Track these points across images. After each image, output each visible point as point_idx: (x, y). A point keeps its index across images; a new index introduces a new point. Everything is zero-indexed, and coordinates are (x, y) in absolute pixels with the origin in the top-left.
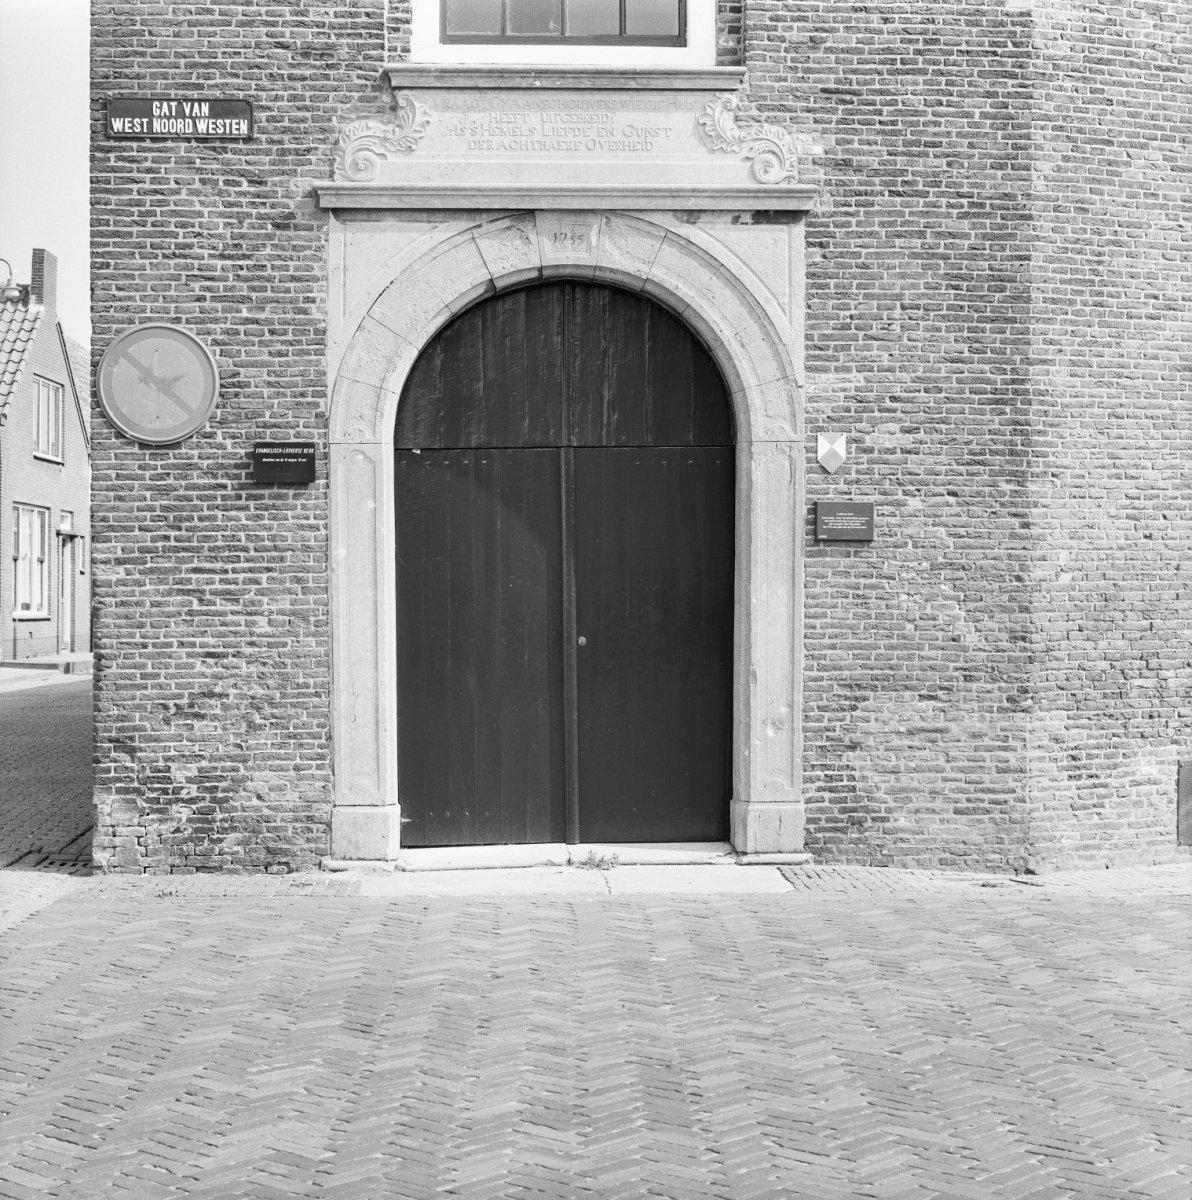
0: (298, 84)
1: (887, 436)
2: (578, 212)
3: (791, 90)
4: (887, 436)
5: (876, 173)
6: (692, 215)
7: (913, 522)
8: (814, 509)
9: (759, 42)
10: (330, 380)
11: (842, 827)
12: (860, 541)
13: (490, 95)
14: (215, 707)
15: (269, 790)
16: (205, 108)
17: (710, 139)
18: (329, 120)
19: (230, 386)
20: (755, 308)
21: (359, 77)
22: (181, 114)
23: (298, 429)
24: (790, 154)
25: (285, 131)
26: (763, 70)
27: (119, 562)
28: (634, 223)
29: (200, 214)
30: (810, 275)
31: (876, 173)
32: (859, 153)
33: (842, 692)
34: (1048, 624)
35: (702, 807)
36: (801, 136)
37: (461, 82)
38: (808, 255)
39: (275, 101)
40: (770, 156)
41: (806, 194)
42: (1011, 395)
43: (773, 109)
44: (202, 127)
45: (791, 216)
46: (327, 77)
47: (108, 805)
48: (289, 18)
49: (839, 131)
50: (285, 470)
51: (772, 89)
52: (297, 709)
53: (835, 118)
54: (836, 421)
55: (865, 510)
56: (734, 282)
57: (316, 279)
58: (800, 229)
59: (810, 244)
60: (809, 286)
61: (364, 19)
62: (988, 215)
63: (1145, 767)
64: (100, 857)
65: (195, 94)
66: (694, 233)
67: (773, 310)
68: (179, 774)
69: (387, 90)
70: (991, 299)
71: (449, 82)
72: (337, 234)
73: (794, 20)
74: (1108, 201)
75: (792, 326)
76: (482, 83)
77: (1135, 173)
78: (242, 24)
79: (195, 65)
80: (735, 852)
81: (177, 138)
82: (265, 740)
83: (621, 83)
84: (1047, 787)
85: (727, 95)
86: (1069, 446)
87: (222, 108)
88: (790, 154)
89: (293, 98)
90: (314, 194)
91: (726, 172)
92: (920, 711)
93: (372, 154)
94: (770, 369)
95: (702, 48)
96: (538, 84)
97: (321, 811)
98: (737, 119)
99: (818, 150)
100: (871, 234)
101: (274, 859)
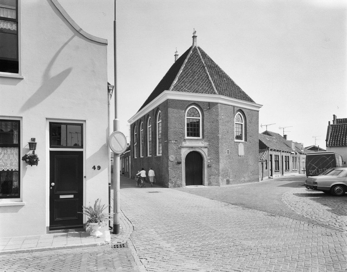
1: (212, 161)
2: (195, 147)
4: (212, 161)
6: (201, 148)
7: (214, 165)
8: (208, 165)
9: (205, 137)
11: (210, 184)
12: (210, 167)
15: (179, 182)
17: (202, 143)
19: (176, 158)
20: (205, 153)
23: (180, 160)
26: (205, 139)
34: (220, 171)
35: (201, 183)
39: (179, 141)
42: (218, 158)
43: (205, 141)
45: (207, 148)
47: (170, 184)
50: (179, 163)
52: (180, 177)
54: (209, 160)
55: (211, 165)
56: (203, 151)
63: (225, 180)
64: (169, 187)
66: (202, 149)
68: (173, 182)
69: (185, 140)
70: (217, 153)
71: (188, 139)
74: (223, 147)
75: (207, 154)
80: (204, 185)
84: (220, 181)
86: (221, 161)
87: (176, 141)
88: (206, 144)
90: (181, 146)
91: (203, 145)
92: (213, 177)
93: (185, 144)
94: (205, 157)
95: (201, 137)
97: (181, 184)
101: (179, 187)
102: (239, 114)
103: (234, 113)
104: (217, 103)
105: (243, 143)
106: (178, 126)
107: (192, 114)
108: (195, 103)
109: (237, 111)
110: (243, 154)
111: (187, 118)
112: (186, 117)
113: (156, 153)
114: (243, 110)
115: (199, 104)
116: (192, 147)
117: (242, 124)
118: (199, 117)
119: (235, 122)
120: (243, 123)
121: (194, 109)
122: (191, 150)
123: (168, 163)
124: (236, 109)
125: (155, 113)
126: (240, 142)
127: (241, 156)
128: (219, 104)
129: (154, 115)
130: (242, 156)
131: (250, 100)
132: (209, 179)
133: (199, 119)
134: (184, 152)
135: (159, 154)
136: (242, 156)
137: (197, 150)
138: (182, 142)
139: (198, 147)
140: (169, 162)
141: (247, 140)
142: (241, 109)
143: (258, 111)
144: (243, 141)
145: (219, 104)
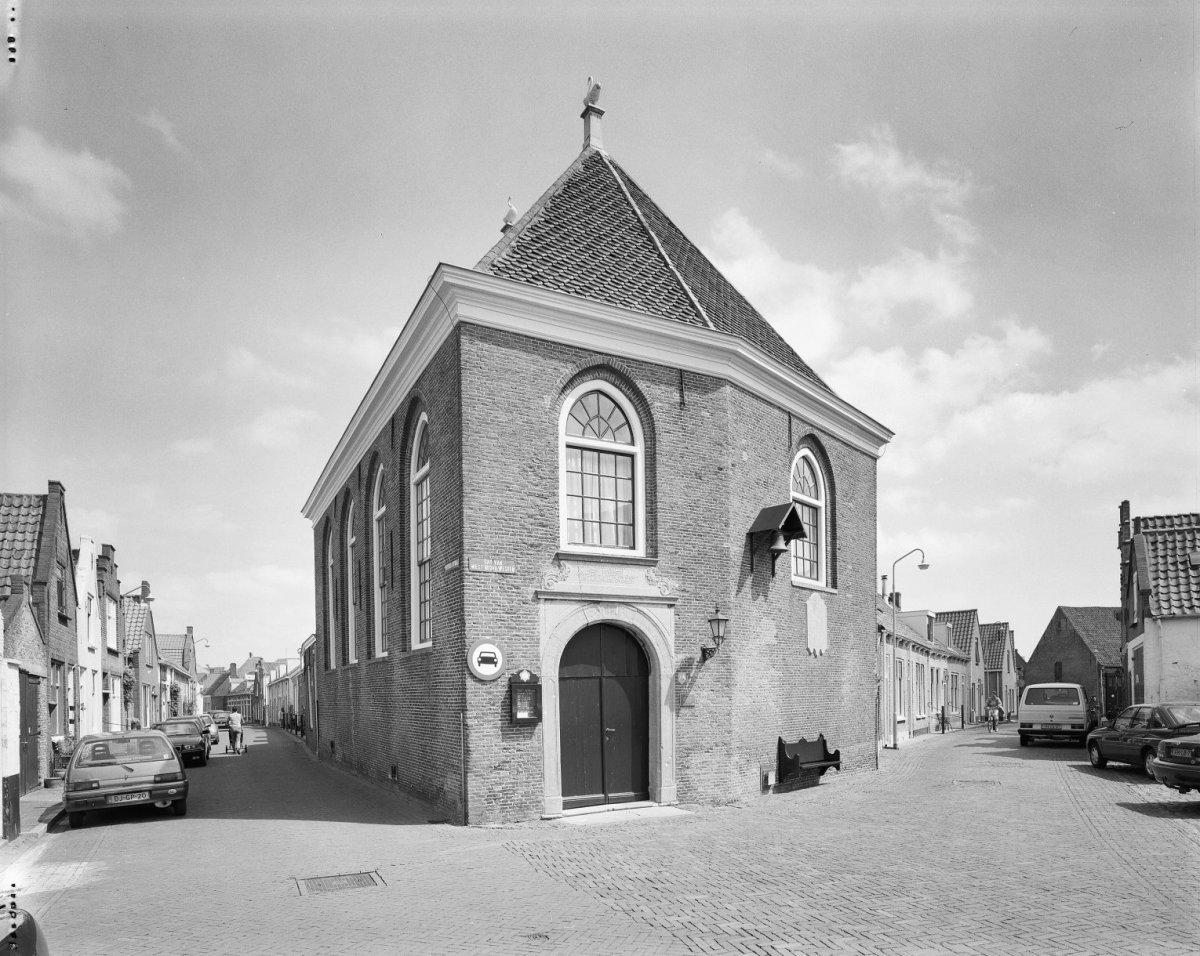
10: (541, 655)
14: (507, 766)
20: (661, 633)
24: (668, 586)
27: (475, 718)
33: (684, 753)
35: (644, 791)
41: (676, 599)
56: (656, 625)
58: (672, 610)
67: (667, 635)
72: (543, 607)
75: (671, 640)
82: (523, 777)
88: (668, 586)
91: (654, 592)
95: (640, 552)
103: (790, 447)
104: (719, 382)
105: (823, 594)
107: (594, 423)
110: (826, 648)
113: (406, 637)
114: (824, 440)
116: (594, 600)
118: (633, 443)
120: (821, 503)
121: (602, 397)
123: (464, 684)
124: (800, 430)
125: (399, 433)
127: (818, 654)
128: (728, 389)
129: (398, 441)
130: (821, 655)
132: (682, 766)
133: (632, 456)
134: (557, 626)
135: (421, 641)
136: (821, 655)
139: (626, 602)
140: (469, 682)
141: (839, 583)
142: (816, 432)
143: (875, 459)
145: (728, 389)
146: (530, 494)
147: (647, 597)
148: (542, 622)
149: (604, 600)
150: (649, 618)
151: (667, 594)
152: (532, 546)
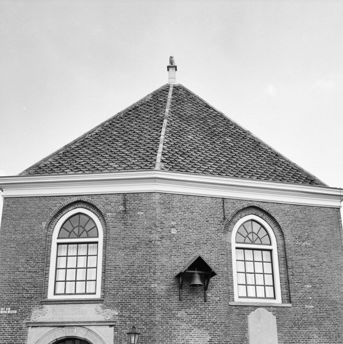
0: (26, 304)
3: (112, 302)
5: (127, 317)
13: (59, 305)
16: (10, 309)
18: (31, 310)
21: (37, 302)
22: (5, 310)
24: (111, 314)
25: (23, 312)
28: (83, 328)
29: (7, 328)
30: (114, 337)
31: (127, 317)
32: (124, 314)
36: (114, 311)
37: (54, 303)
38: (114, 333)
40: (108, 315)
41: (115, 322)
43: (108, 306)
44: (9, 312)
46: (31, 303)
48: (25, 292)
49: (121, 310)
51: (109, 302)
53: (120, 307)
57: (26, 339)
58: (113, 328)
59: (115, 331)
60: (114, 339)
61: (38, 292)
62: (148, 325)
65: (8, 306)
72: (30, 330)
73: (113, 290)
76: (57, 303)
77: (179, 315)
78: (17, 294)
79: (9, 301)
81: (4, 314)
83: (82, 302)
85: (100, 304)
88: (111, 314)
89: (25, 306)
96: (67, 303)
98: (102, 308)
99: (117, 313)
100: (126, 329)
102: (252, 220)
106: (26, 266)
107: (76, 230)
108: (79, 202)
109: (240, 212)
111: (58, 244)
112: (55, 240)
115: (94, 203)
116: (61, 325)
117: (271, 251)
119: (234, 245)
120: (274, 247)
122: (61, 334)
126: (256, 307)
131: (311, 181)
137: (79, 333)
138: (30, 312)
142: (255, 204)
144: (278, 301)
146: (29, 272)
147: (93, 322)
148: (28, 340)
149: (66, 325)
150: (96, 334)
151: (109, 318)
152: (28, 298)
